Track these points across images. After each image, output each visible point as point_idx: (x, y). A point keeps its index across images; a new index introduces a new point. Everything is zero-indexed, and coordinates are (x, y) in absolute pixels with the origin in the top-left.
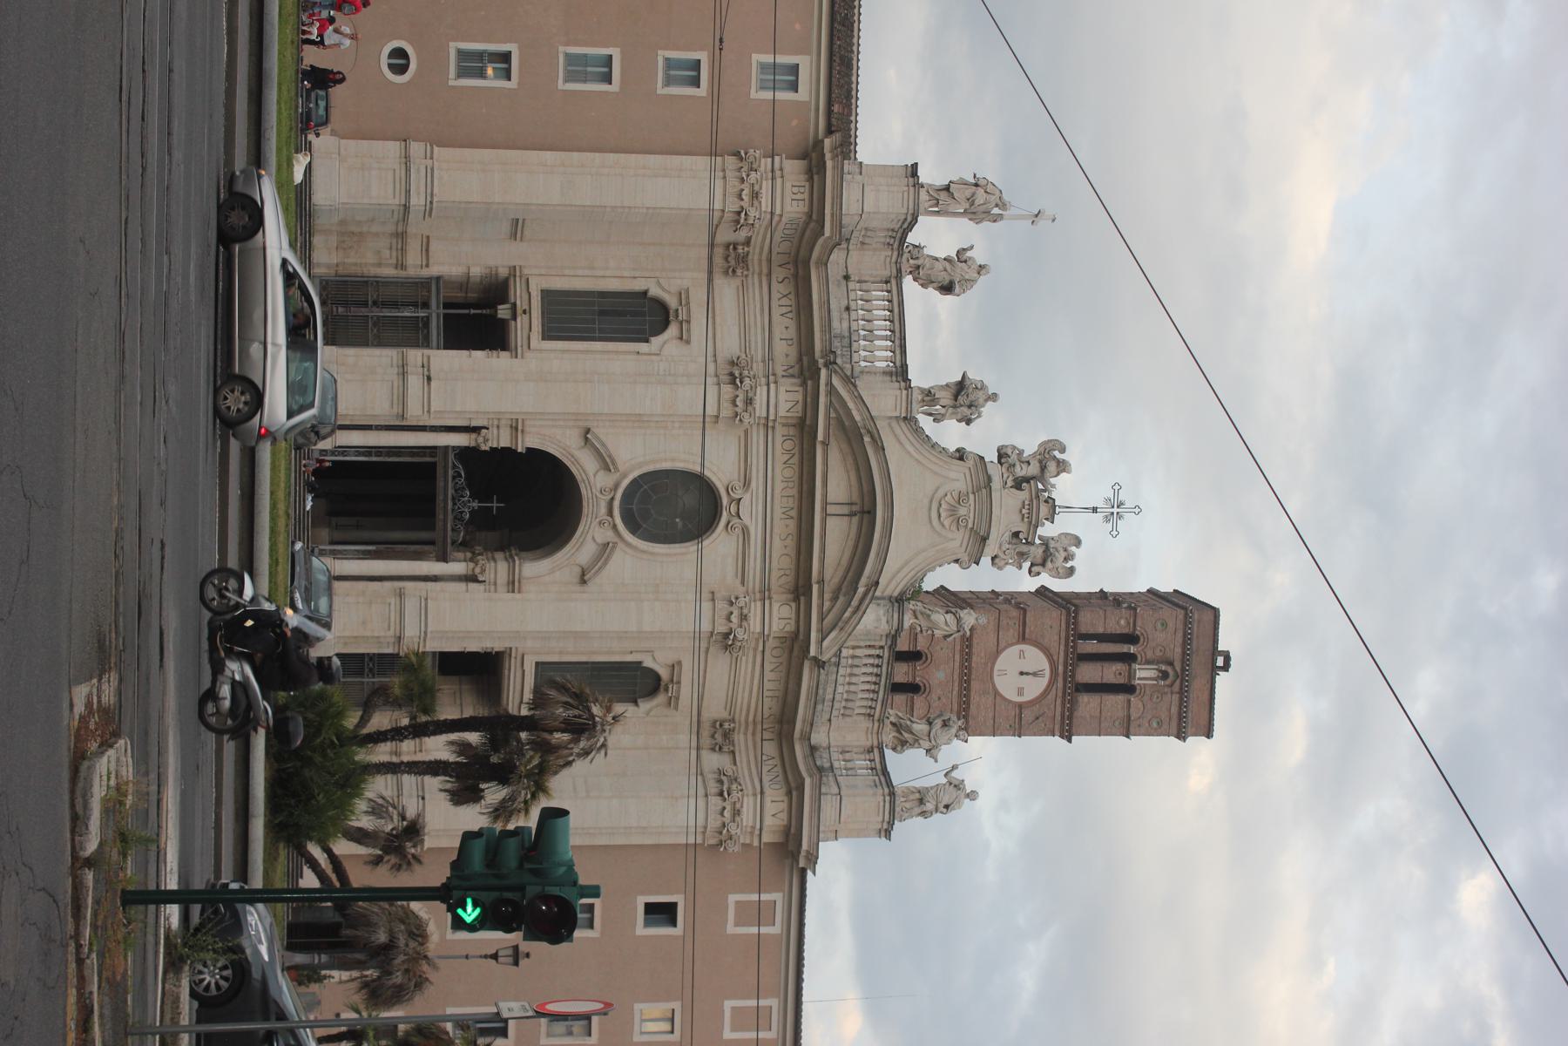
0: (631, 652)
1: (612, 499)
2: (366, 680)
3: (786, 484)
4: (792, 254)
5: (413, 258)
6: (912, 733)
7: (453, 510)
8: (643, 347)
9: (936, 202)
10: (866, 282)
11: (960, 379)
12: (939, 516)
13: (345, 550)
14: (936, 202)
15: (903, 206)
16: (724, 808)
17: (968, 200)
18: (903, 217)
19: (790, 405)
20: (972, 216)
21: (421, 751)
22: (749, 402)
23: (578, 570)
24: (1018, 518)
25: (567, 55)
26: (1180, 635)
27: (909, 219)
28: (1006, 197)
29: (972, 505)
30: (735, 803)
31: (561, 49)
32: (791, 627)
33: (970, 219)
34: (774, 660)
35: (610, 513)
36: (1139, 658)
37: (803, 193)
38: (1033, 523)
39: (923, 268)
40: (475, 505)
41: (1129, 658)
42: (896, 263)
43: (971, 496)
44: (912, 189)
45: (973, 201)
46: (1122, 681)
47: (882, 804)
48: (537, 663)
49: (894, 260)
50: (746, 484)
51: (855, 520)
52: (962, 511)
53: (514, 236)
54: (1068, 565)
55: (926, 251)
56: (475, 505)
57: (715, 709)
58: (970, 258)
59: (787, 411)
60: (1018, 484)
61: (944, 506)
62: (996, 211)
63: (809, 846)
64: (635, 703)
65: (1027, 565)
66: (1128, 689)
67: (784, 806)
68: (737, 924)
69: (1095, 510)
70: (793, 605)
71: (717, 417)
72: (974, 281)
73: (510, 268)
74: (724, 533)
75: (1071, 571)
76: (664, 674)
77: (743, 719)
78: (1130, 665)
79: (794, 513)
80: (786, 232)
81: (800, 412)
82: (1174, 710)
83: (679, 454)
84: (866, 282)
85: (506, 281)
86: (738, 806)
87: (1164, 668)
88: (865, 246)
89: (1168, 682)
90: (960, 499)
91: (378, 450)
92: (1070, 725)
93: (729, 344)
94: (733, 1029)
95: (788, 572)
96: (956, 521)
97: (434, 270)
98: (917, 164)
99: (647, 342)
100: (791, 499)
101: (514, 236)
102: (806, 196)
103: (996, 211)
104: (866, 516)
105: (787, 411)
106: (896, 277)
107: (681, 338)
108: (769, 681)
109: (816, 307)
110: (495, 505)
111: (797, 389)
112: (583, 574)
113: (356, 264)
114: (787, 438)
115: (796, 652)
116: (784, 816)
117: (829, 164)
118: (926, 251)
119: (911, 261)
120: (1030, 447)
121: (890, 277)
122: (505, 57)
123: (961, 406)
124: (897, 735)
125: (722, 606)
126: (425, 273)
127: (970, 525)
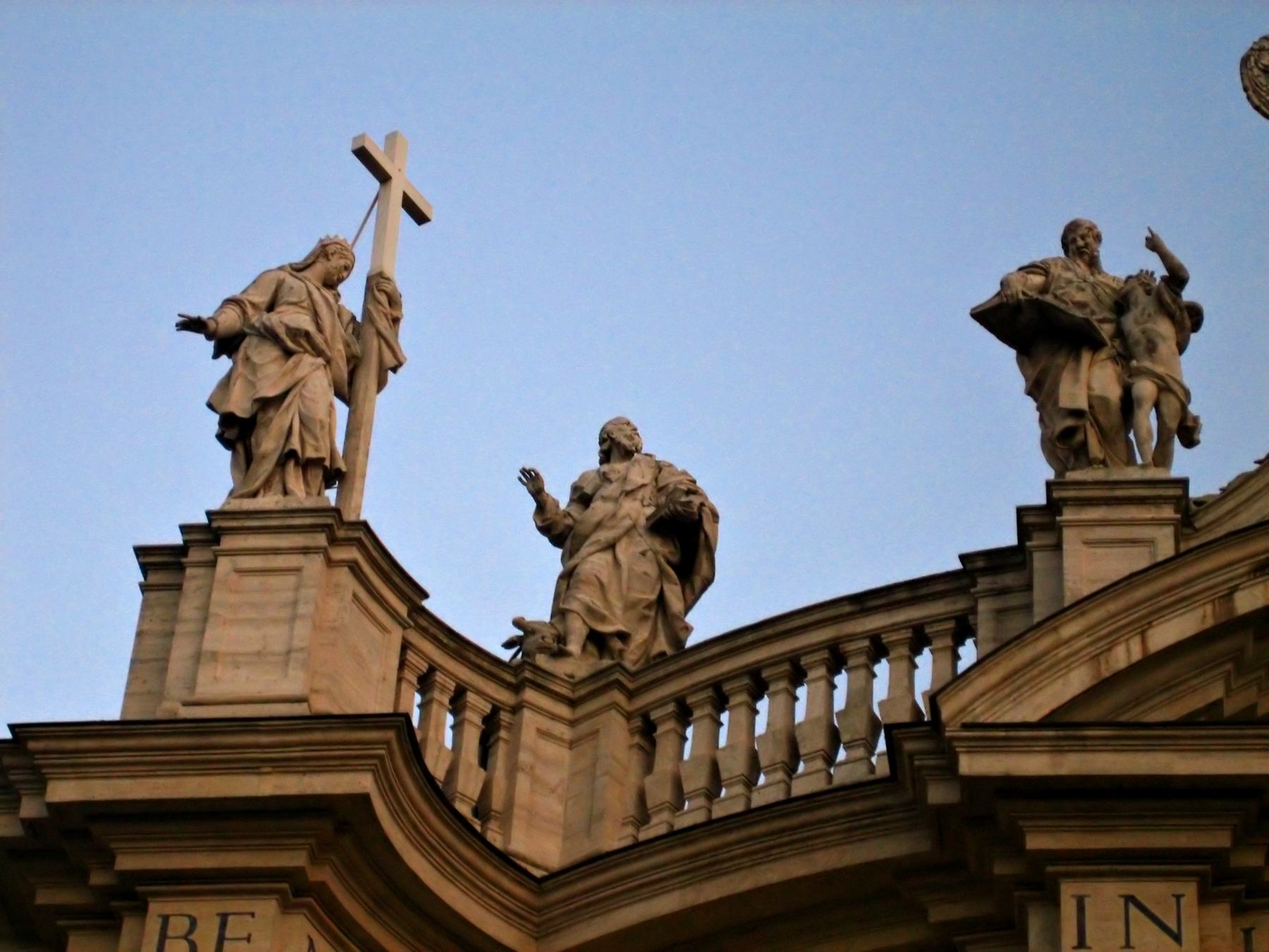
9: (291, 464)
10: (642, 797)
11: (1011, 353)
14: (291, 464)
15: (298, 570)
17: (288, 353)
18: (344, 575)
20: (368, 376)
27: (353, 554)
28: (299, 254)
33: (381, 384)
37: (193, 922)
39: (603, 619)
42: (572, 703)
44: (228, 542)
45: (295, 333)
49: (563, 710)
55: (540, 612)
58: (576, 488)
59: (1177, 938)
62: (352, 296)
72: (659, 467)
81: (1178, 887)
84: (642, 797)
88: (497, 802)
98: (140, 551)
102: (206, 910)
103: (352, 296)
105: (1177, 938)
106: (631, 695)
109: (712, 891)
111: (1068, 908)
117: (63, 791)
118: (540, 612)
119: (574, 647)
121: (629, 716)
123: (1120, 334)
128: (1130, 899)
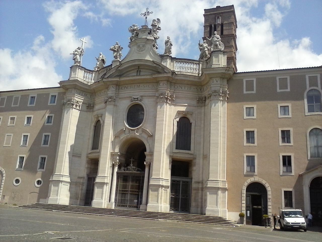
0: (174, 124)
1: (131, 129)
2: (180, 197)
3: (132, 88)
4: (91, 94)
5: (81, 181)
6: (203, 53)
7: (132, 171)
8: (102, 125)
12: (142, 51)
13: (140, 201)
16: (214, 95)
19: (113, 88)
21: (202, 182)
22: (111, 98)
23: (149, 138)
24: (144, 33)
25: (43, 145)
26: (210, 16)
29: (140, 43)
30: (212, 92)
31: (42, 146)
32: (165, 82)
34: (178, 88)
35: (134, 130)
36: (215, 24)
38: (145, 30)
40: (132, 165)
41: (215, 26)
43: (138, 44)
46: (220, 27)
47: (215, 54)
48: (177, 148)
50: (131, 97)
51: (141, 70)
52: (141, 46)
53: (80, 157)
54: (157, 20)
56: (132, 165)
57: (194, 102)
60: (137, 35)
61: (140, 50)
63: (224, 70)
64: (191, 124)
65: (158, 31)
66: (222, 25)
67: (214, 80)
68: (253, 90)
69: (146, 18)
70: (160, 82)
71: (114, 105)
73: (87, 158)
74: (142, 101)
75: (158, 19)
76: (181, 116)
77: (197, 96)
78: (216, 25)
79: (138, 85)
80: (83, 95)
82: (227, 14)
83: (124, 114)
85: (89, 158)
86: (213, 91)
87: (216, 18)
89: (219, 16)
90: (139, 46)
91: (117, 190)
92: (229, 35)
93: (103, 105)
94: (287, 89)
95: (153, 85)
96: (144, 47)
97: (85, 175)
99: (101, 124)
100: (135, 86)
101: (80, 157)
102: (71, 90)
104: (139, 67)
107: (101, 117)
108: (185, 89)
110: (132, 160)
112: (149, 136)
113: (81, 195)
114: (122, 89)
115: (175, 82)
116: (217, 79)
120: (130, 35)
122: (42, 158)
124: (204, 57)
125: (158, 100)
126: (86, 178)
127: (144, 43)
128: (112, 87)
